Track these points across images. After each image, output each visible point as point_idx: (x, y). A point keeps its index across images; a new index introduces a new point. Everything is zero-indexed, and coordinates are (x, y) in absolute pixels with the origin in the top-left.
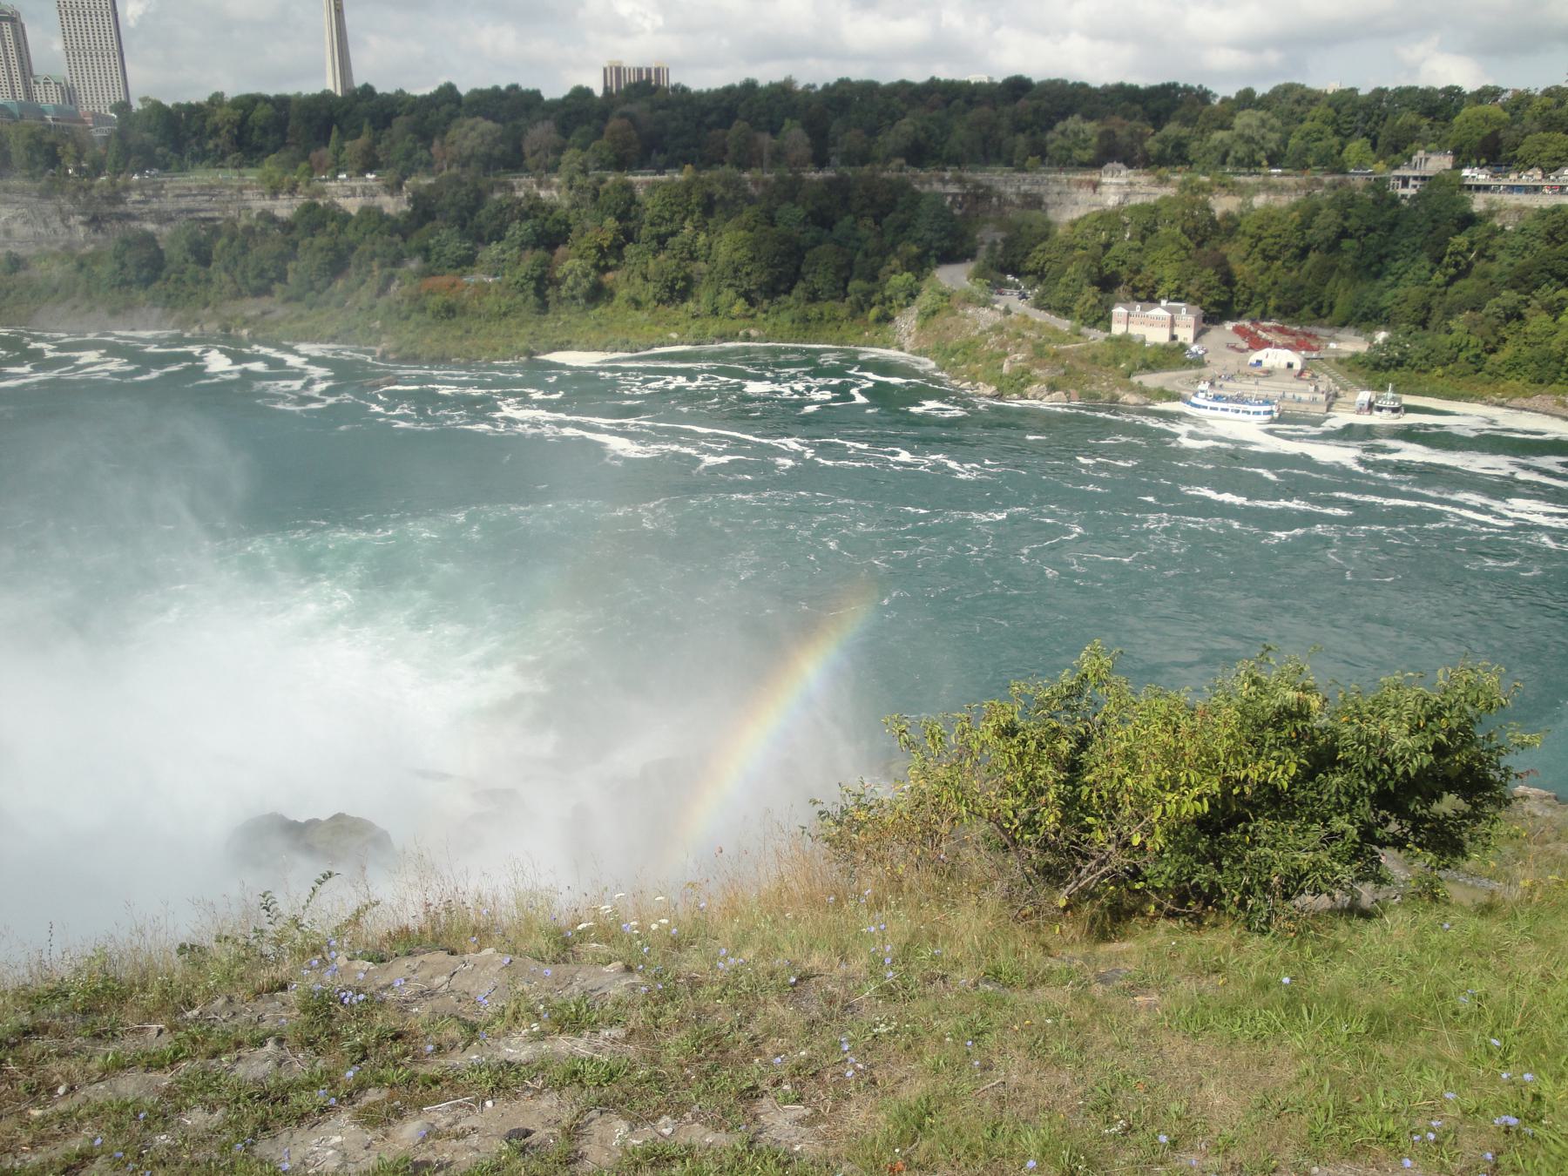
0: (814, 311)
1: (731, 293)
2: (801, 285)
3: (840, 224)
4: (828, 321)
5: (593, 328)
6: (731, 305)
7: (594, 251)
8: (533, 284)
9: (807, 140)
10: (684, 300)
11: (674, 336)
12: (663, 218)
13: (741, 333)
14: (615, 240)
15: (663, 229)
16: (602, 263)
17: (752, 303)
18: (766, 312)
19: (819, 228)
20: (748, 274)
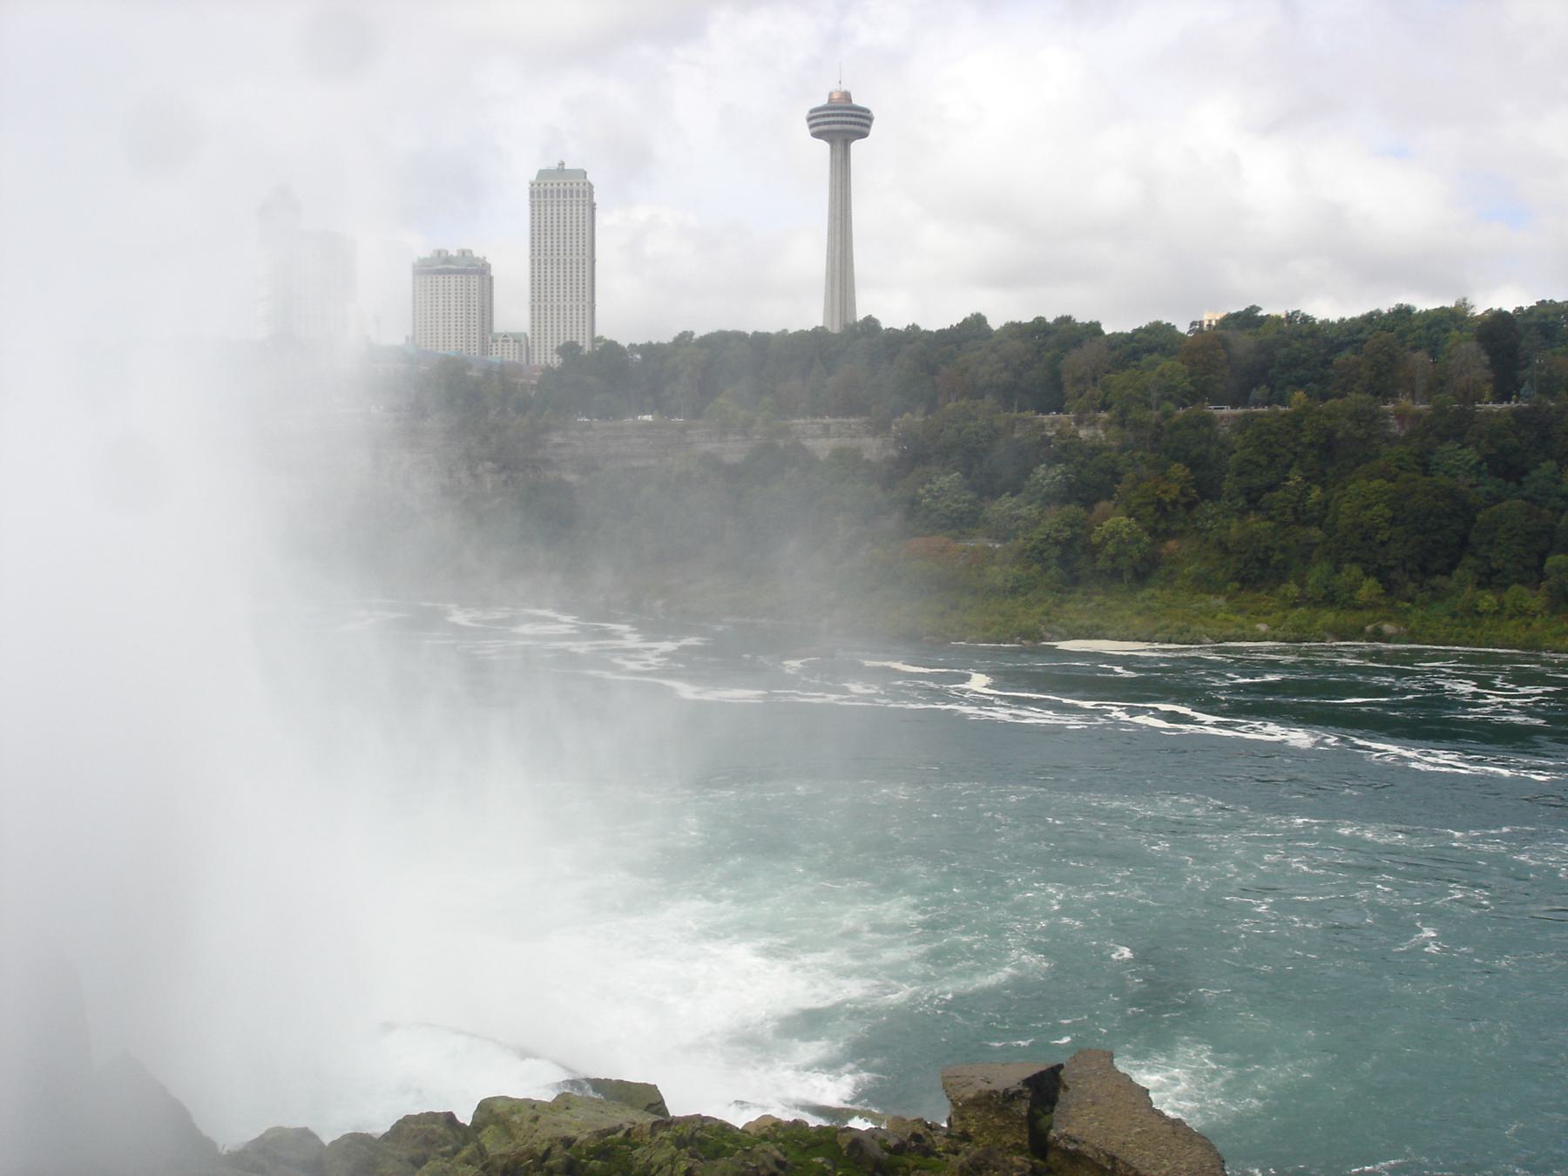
0: (1488, 600)
1: (1356, 570)
2: (1469, 561)
3: (1534, 473)
4: (1511, 617)
5: (1139, 614)
6: (1355, 587)
7: (1151, 509)
8: (1057, 551)
9: (1485, 358)
10: (1282, 580)
11: (1262, 627)
12: (1259, 466)
13: (1369, 628)
14: (1183, 493)
15: (1256, 482)
16: (1162, 525)
17: (1389, 587)
18: (1410, 600)
19: (1500, 480)
20: (1383, 543)
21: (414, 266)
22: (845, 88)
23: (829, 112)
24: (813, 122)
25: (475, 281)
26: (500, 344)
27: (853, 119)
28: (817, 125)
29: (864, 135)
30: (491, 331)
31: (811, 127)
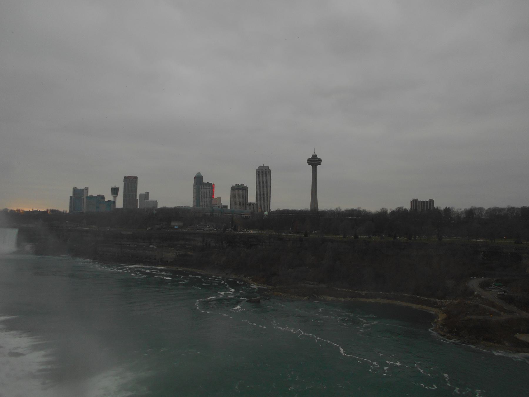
21: (231, 187)
22: (316, 154)
23: (311, 160)
24: (309, 161)
25: (245, 190)
26: (249, 205)
27: (318, 161)
28: (309, 162)
29: (320, 164)
30: (248, 201)
31: (308, 163)
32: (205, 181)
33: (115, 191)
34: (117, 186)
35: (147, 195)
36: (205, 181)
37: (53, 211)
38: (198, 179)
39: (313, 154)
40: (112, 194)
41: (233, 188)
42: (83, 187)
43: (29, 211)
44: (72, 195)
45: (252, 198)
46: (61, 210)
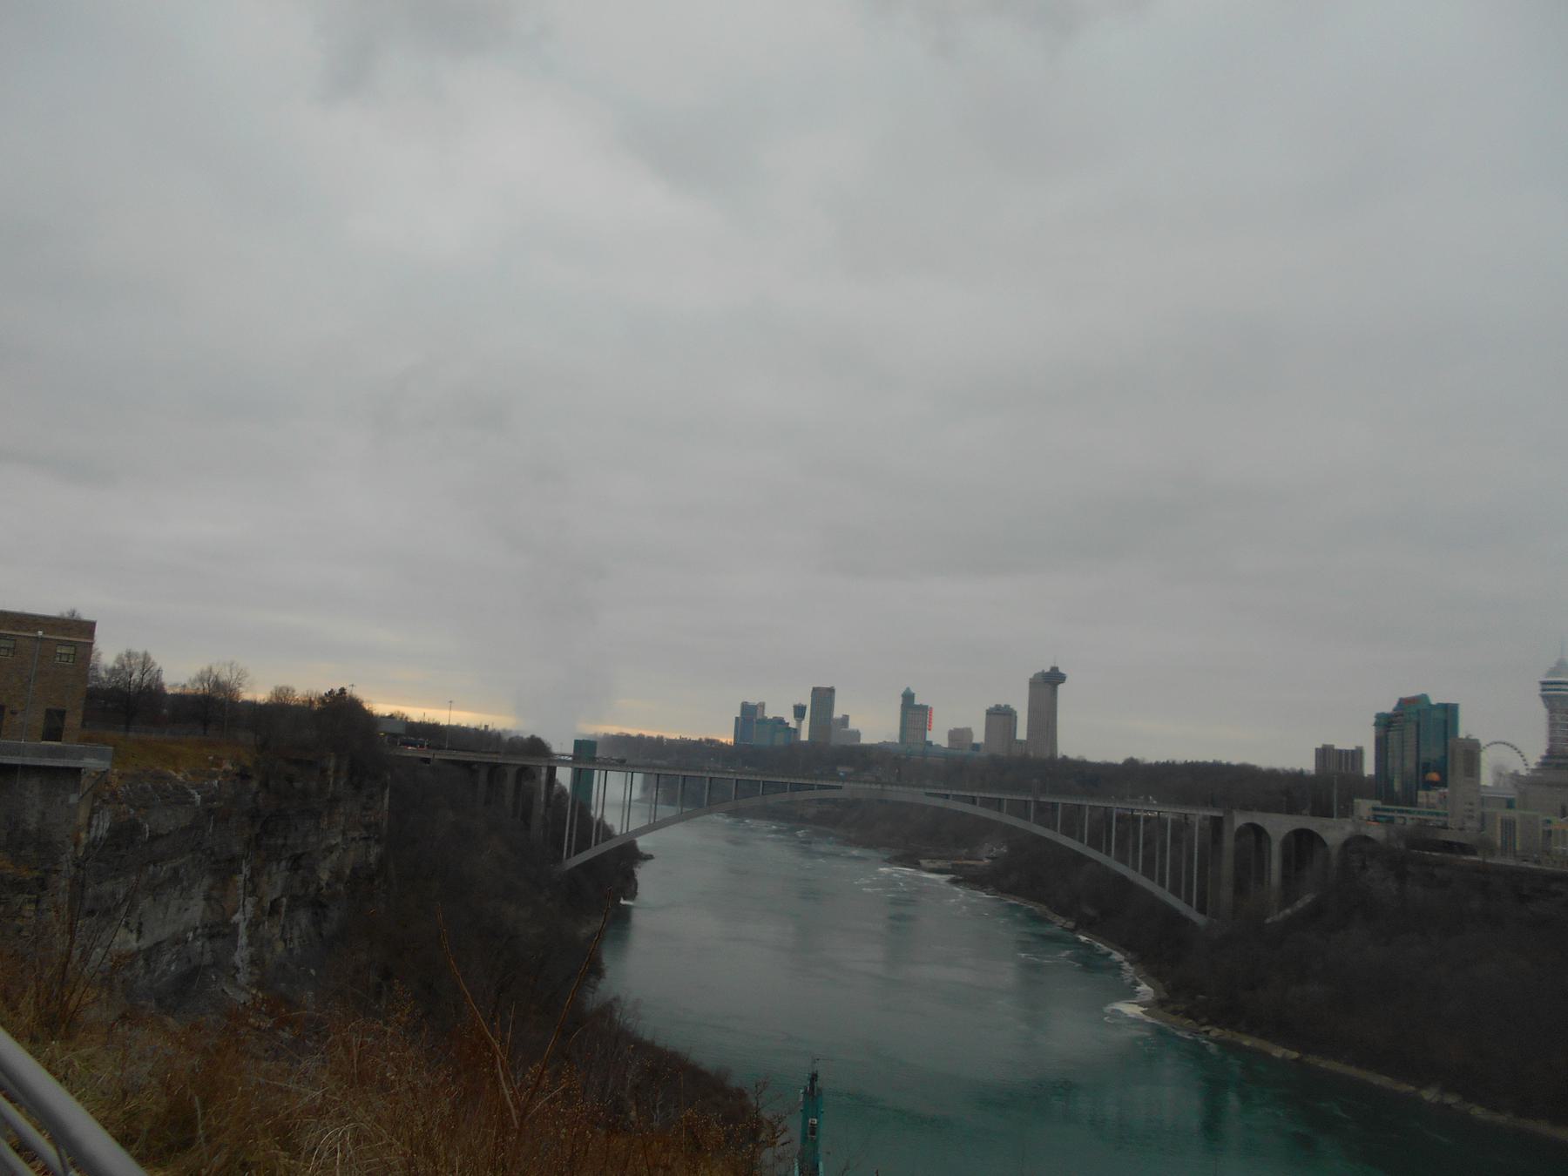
32: (917, 702)
33: (799, 711)
34: (804, 703)
35: (845, 720)
36: (917, 702)
37: (708, 741)
38: (908, 698)
39: (1053, 665)
40: (795, 716)
41: (990, 713)
42: (756, 703)
43: (676, 740)
44: (738, 716)
45: (1022, 733)
46: (723, 740)
